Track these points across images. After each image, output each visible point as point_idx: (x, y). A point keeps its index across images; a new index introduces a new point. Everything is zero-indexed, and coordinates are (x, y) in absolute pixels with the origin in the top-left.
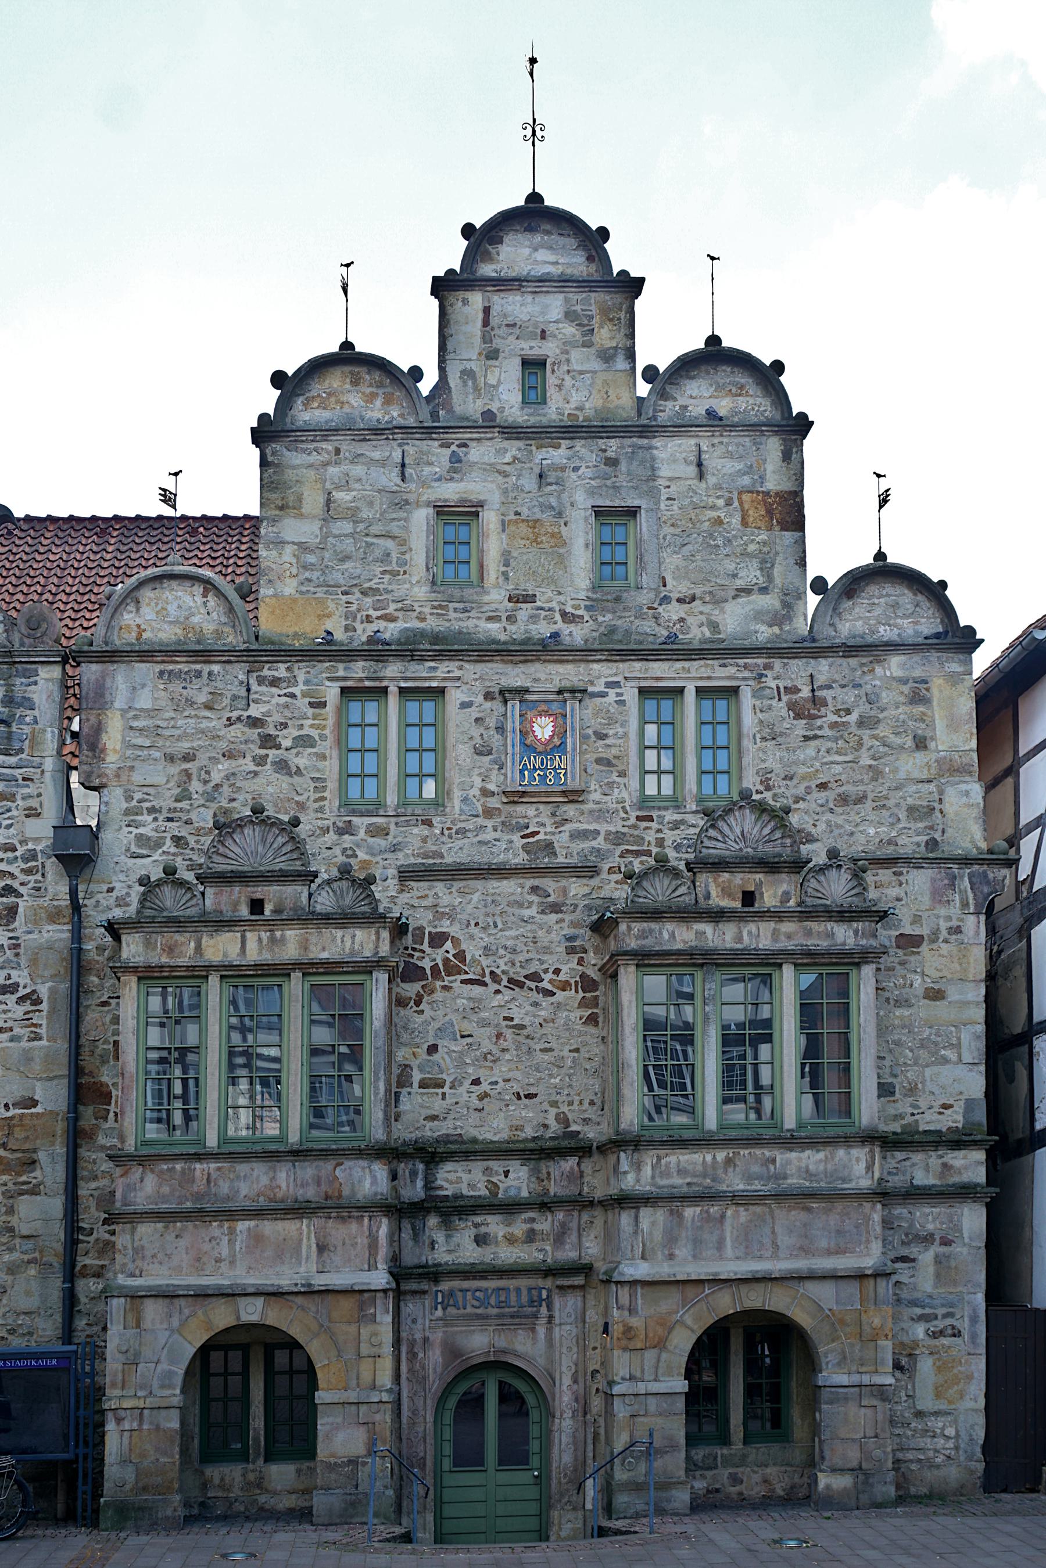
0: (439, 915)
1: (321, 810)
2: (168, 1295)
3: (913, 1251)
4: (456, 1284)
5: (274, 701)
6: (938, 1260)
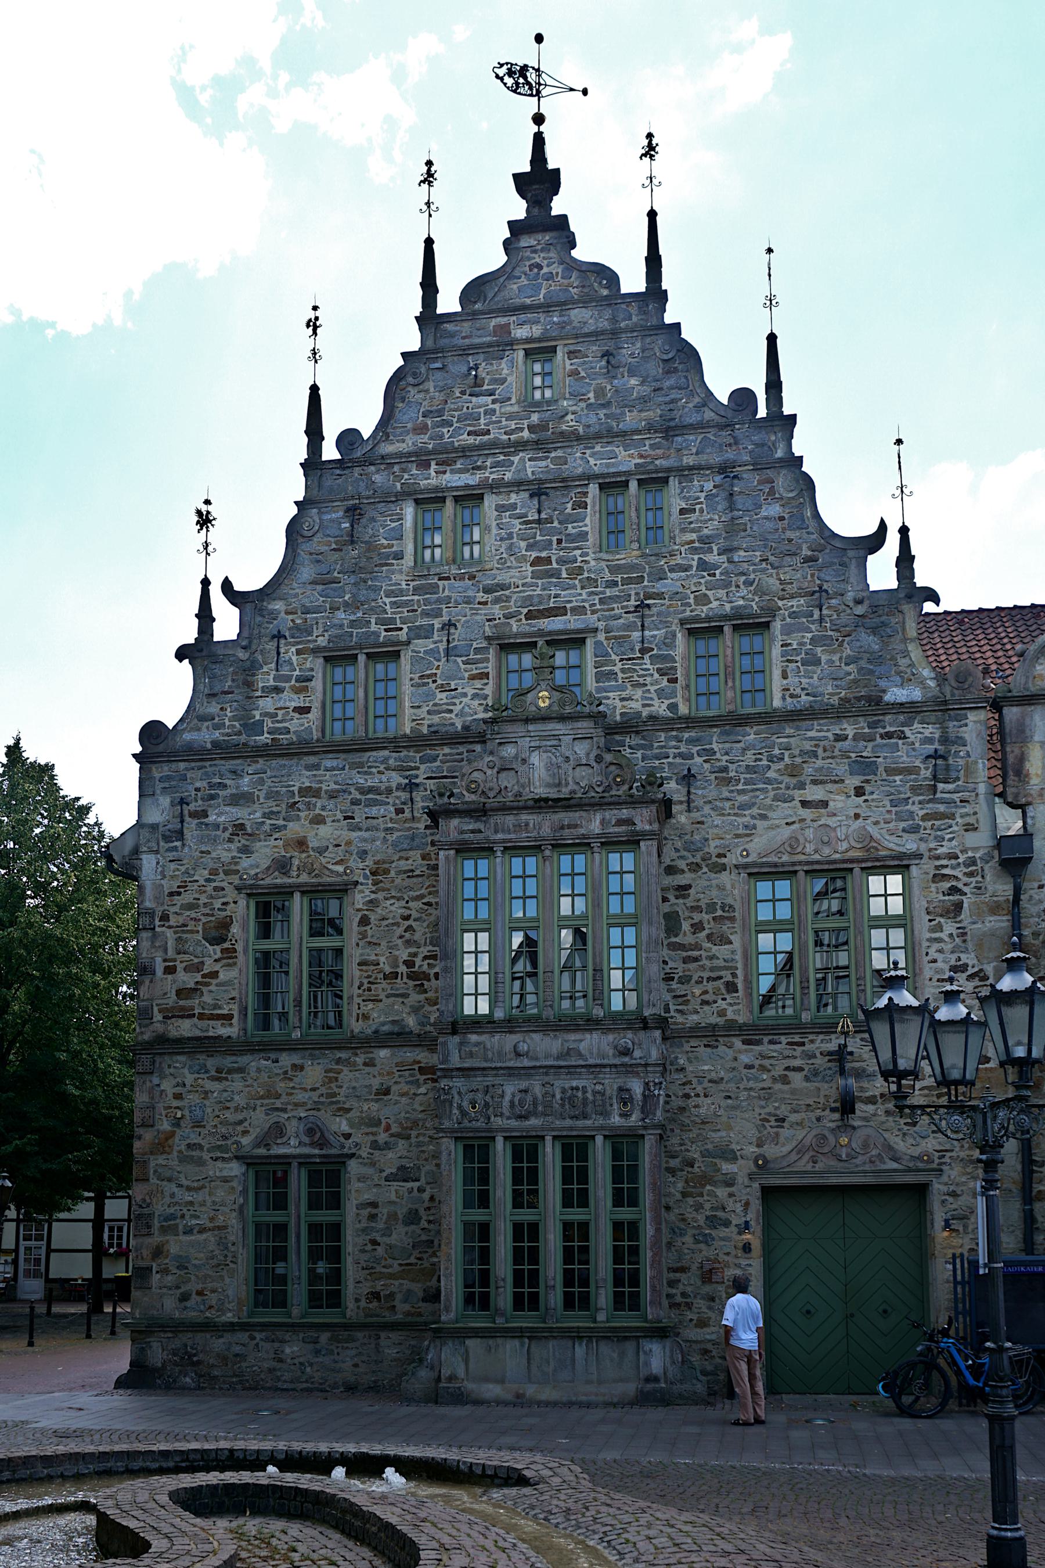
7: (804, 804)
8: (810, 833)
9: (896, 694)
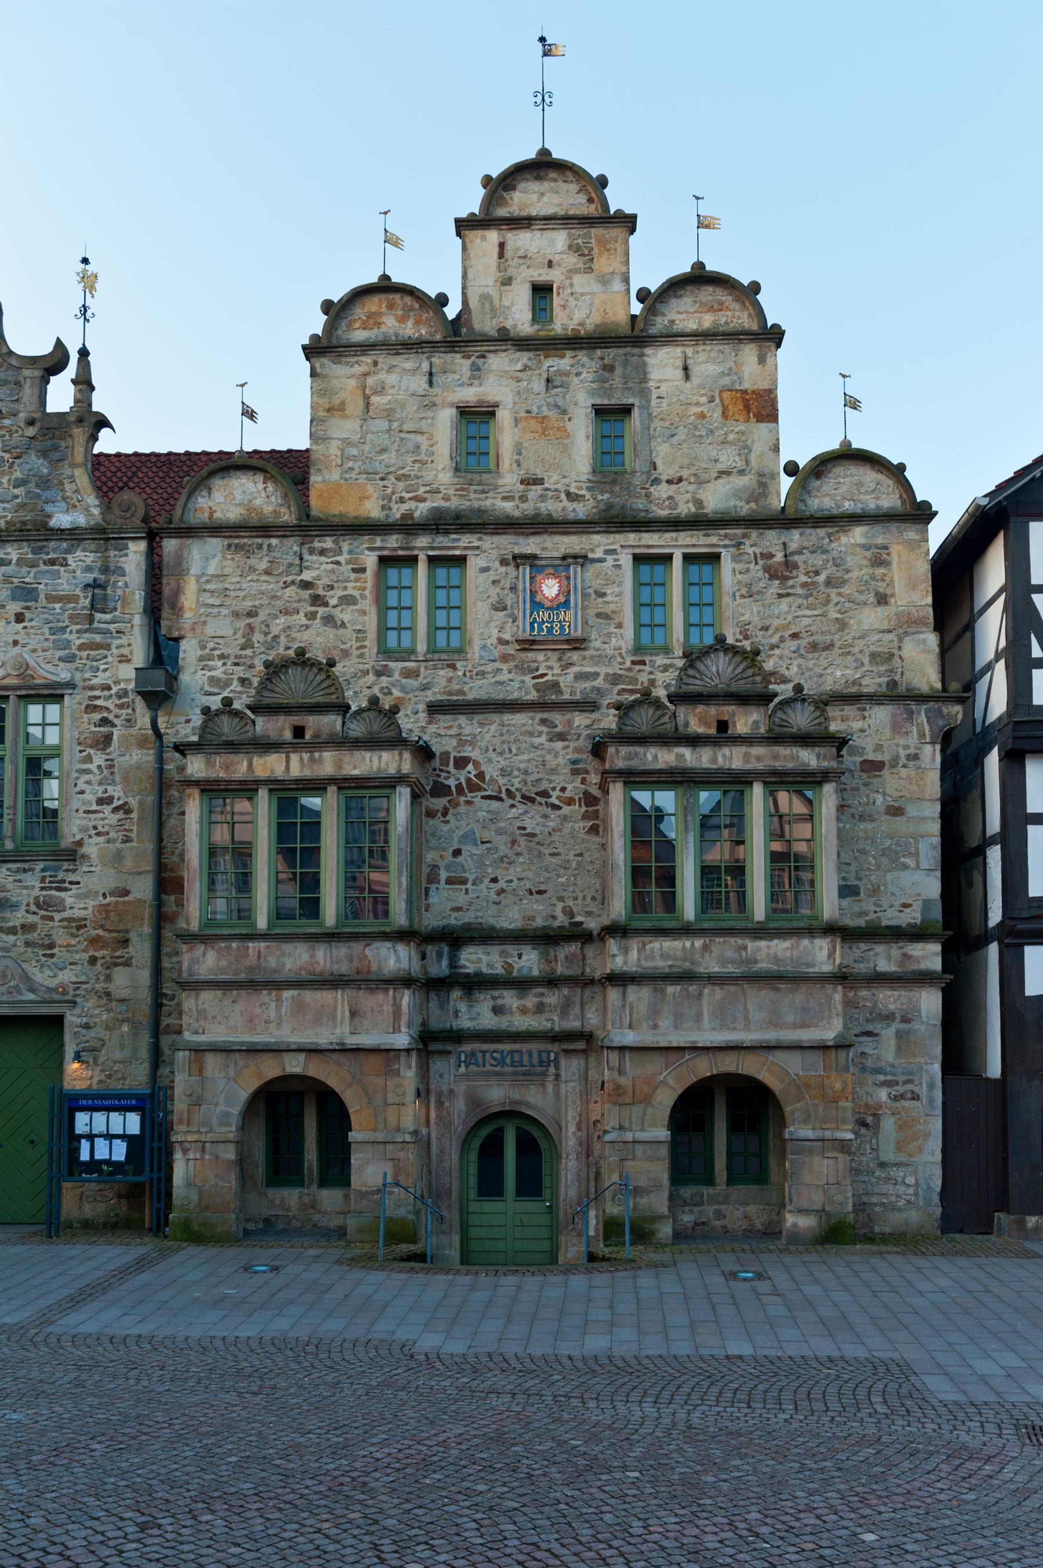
0: (462, 743)
1: (362, 656)
2: (225, 1050)
3: (877, 1027)
4: (477, 1046)
5: (323, 567)
6: (899, 1035)
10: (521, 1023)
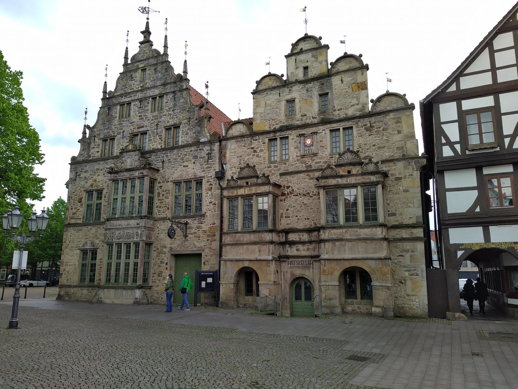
7: (184, 166)
8: (184, 173)
9: (202, 140)
10: (303, 253)
